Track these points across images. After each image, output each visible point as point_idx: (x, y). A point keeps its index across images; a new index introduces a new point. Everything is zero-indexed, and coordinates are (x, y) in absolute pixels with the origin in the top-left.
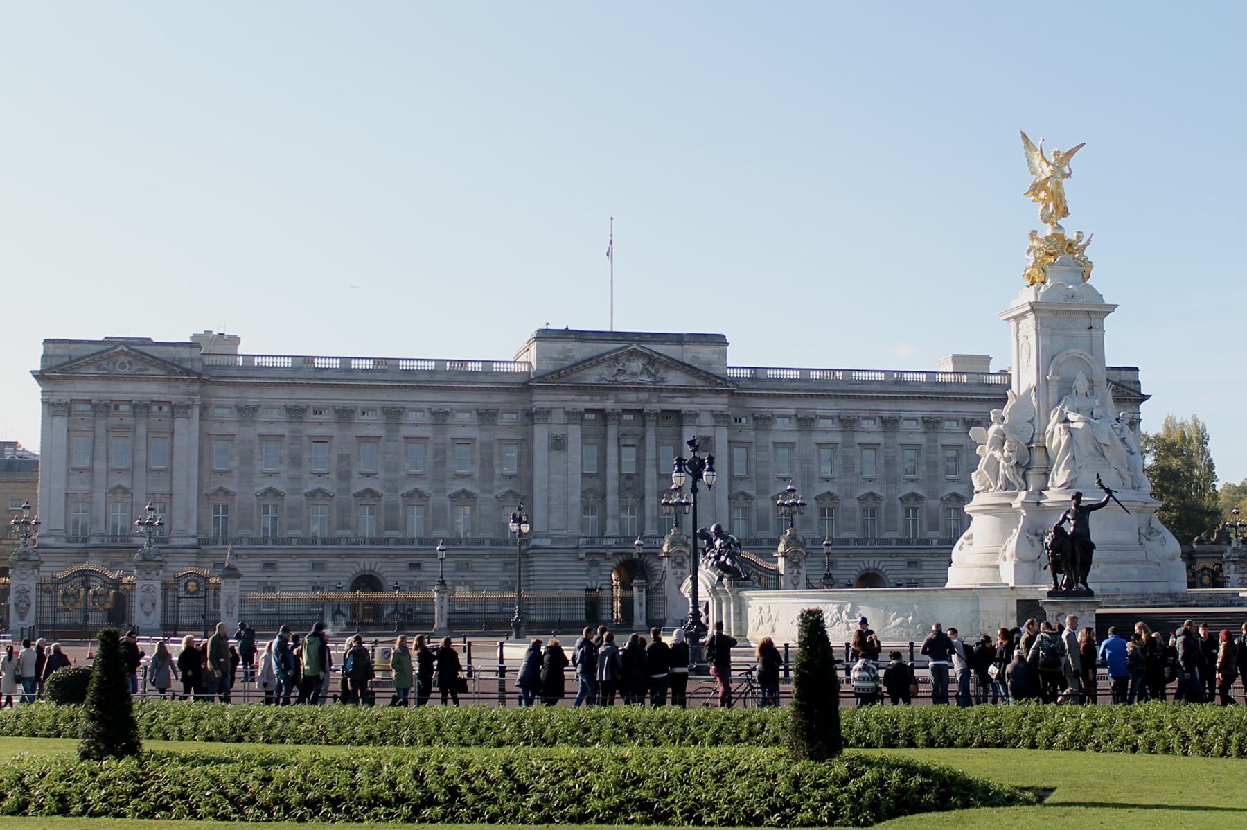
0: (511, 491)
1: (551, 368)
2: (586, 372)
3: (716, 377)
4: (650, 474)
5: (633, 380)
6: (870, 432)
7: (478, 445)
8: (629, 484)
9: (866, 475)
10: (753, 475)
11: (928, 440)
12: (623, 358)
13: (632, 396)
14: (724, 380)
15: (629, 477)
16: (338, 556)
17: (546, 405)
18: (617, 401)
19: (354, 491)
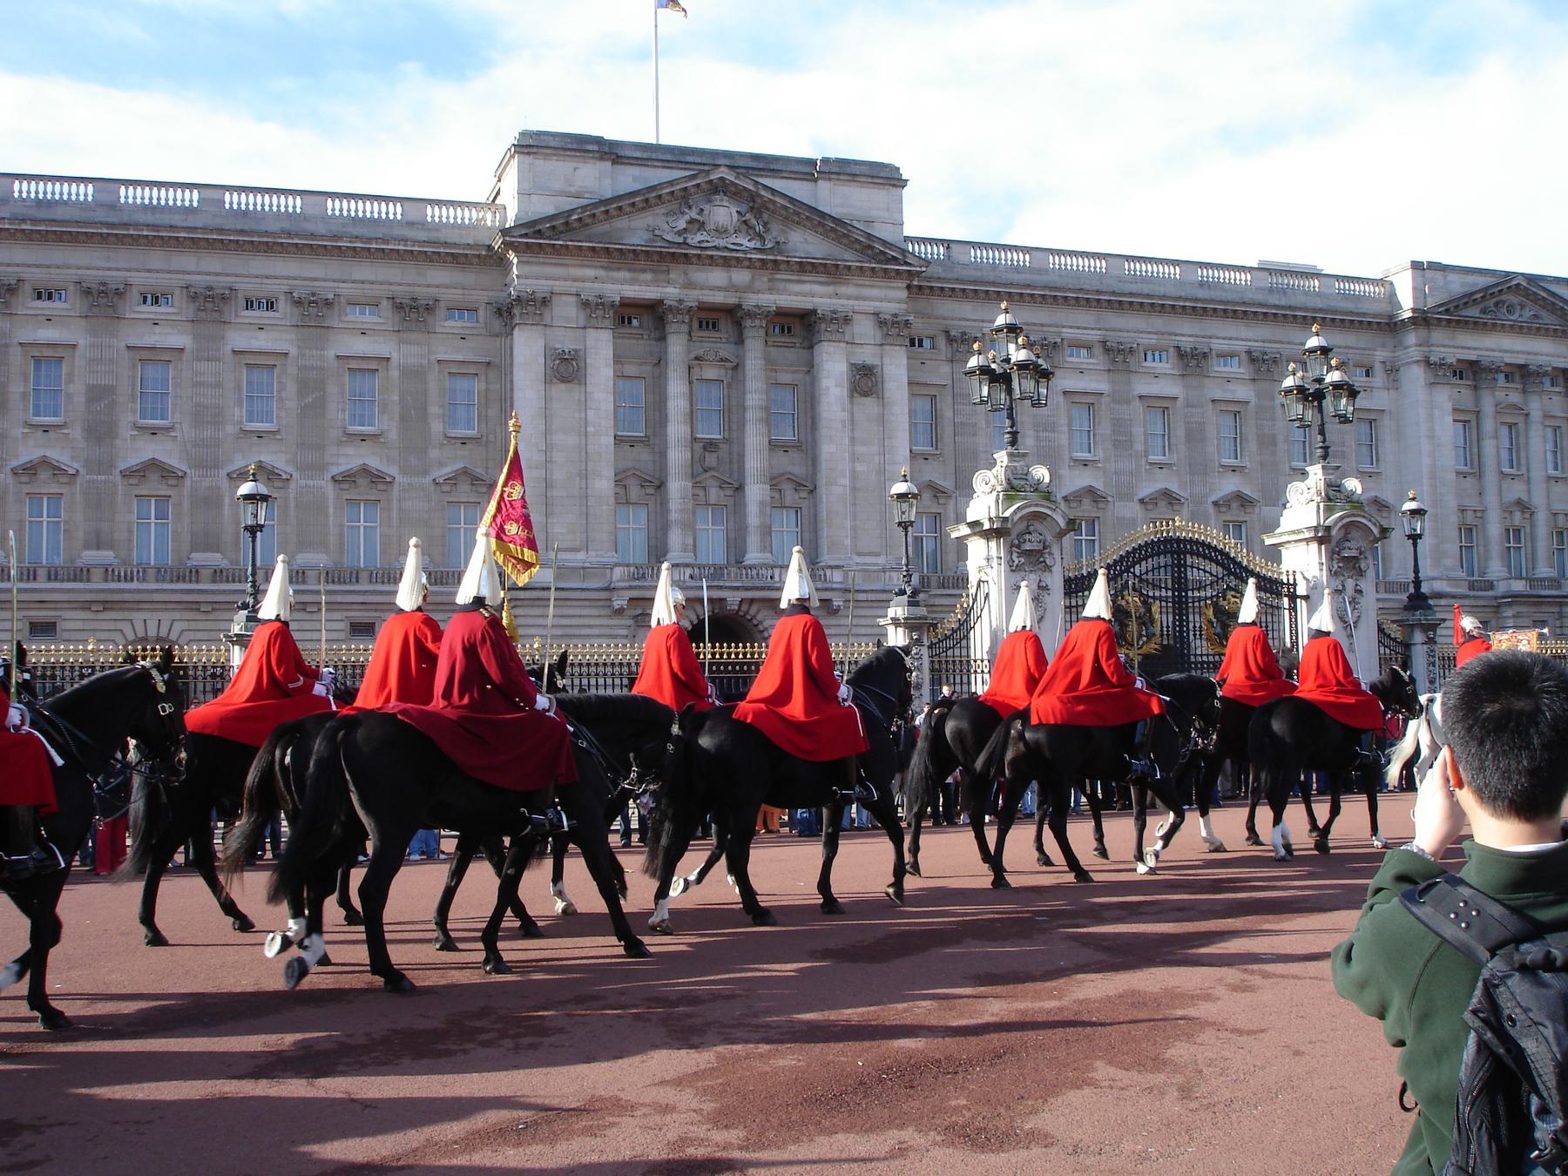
0: (465, 471)
1: (551, 211)
2: (621, 223)
3: (884, 243)
4: (754, 440)
5: (721, 243)
6: (1160, 378)
7: (395, 373)
8: (711, 460)
9: (1152, 458)
10: (948, 449)
11: (1258, 395)
12: (696, 198)
13: (717, 276)
14: (904, 252)
15: (710, 446)
16: (86, 606)
17: (541, 286)
18: (690, 285)
19: (122, 466)
